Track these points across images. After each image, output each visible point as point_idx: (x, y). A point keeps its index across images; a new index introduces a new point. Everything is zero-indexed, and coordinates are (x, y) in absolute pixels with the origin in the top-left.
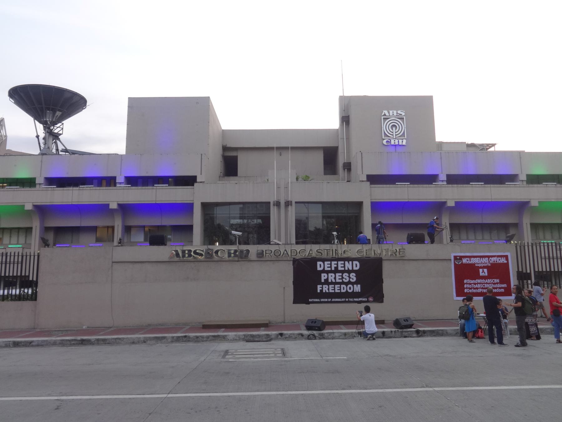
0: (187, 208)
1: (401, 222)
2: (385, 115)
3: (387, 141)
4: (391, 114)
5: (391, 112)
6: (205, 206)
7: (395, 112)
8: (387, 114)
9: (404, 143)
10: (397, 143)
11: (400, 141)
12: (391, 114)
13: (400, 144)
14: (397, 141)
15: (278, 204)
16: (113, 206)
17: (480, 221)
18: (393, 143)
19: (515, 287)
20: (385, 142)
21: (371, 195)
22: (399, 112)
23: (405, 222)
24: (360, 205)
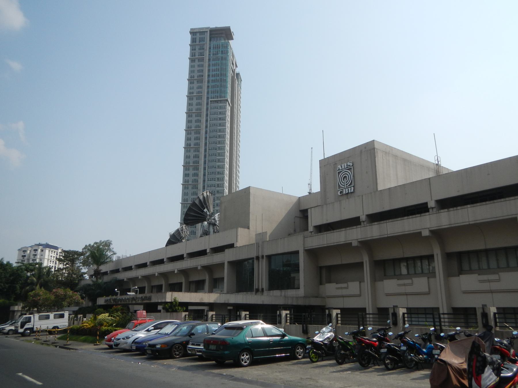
0: (222, 265)
1: (340, 263)
2: (339, 169)
3: (341, 192)
4: (343, 168)
5: (343, 165)
6: (232, 263)
7: (346, 164)
8: (341, 168)
9: (352, 191)
10: (347, 192)
11: (350, 189)
12: (343, 168)
13: (350, 191)
14: (347, 189)
15: (258, 258)
16: (199, 268)
17: (481, 247)
18: (344, 193)
19: (298, 327)
20: (339, 194)
21: (304, 244)
22: (349, 164)
23: (344, 262)
24: (297, 253)
